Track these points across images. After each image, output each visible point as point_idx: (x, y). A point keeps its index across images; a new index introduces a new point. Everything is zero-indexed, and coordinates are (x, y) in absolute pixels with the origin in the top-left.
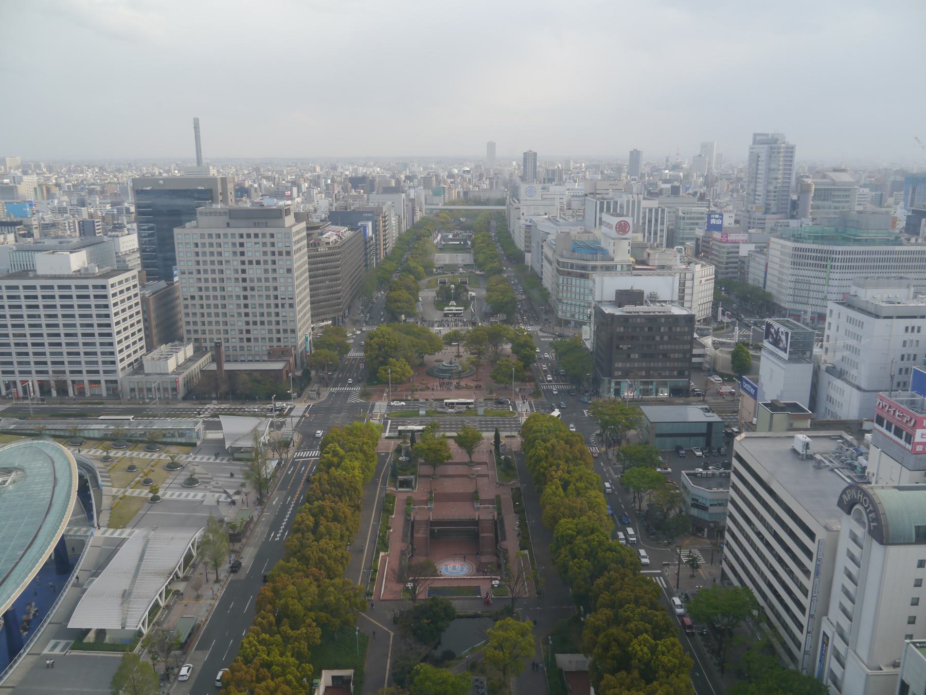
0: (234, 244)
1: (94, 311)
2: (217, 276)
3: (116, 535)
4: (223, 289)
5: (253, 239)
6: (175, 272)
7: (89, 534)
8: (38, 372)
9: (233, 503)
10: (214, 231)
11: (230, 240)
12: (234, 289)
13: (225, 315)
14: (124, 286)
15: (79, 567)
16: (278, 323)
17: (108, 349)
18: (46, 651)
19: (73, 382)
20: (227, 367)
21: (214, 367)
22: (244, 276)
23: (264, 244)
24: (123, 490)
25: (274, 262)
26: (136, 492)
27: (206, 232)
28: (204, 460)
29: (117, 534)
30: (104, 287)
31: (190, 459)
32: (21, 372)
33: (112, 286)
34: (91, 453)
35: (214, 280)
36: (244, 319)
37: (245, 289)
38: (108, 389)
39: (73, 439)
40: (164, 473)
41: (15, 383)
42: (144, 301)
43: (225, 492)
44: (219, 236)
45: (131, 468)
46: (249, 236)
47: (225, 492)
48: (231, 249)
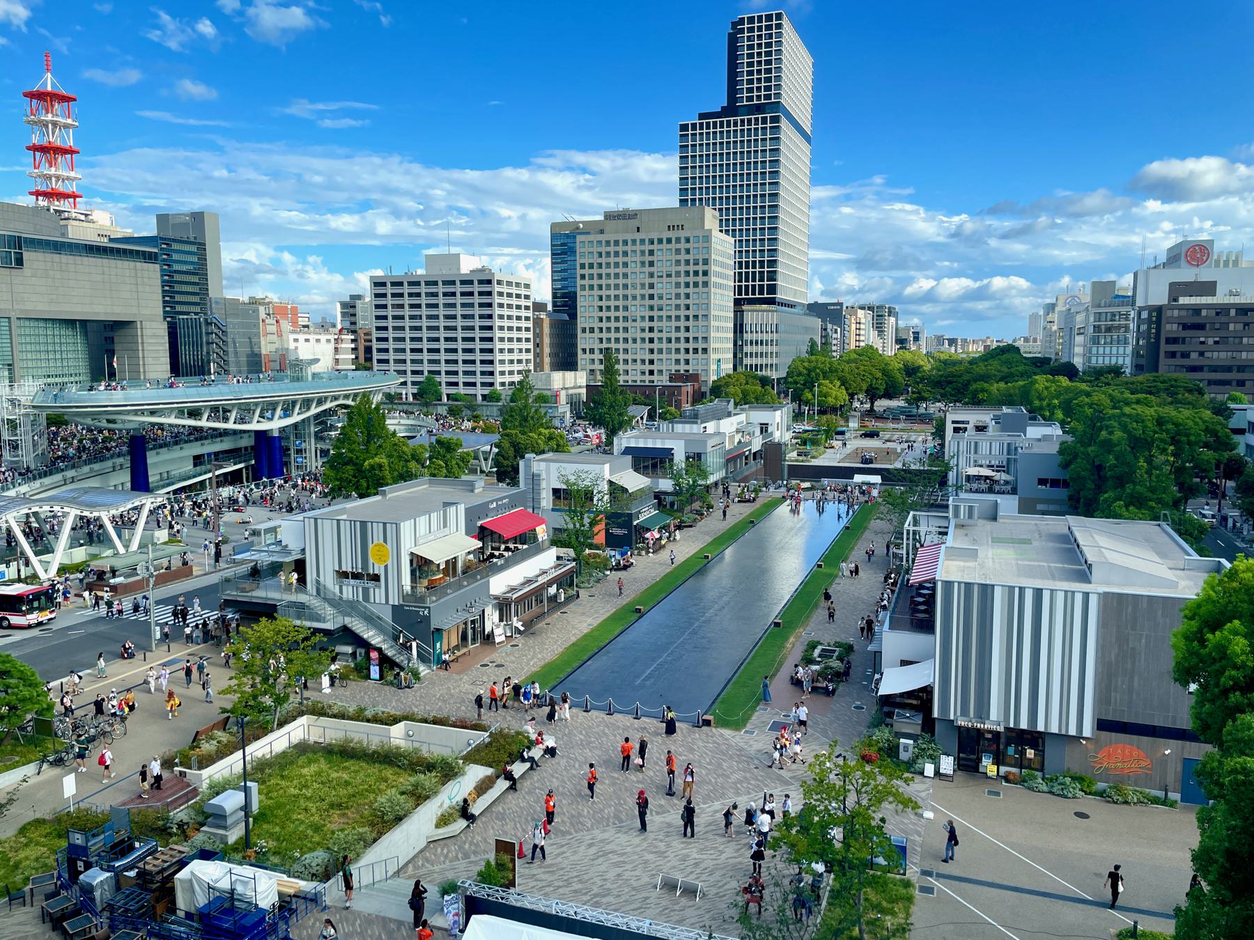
0: (643, 252)
2: (621, 292)
4: (626, 308)
5: (665, 246)
10: (620, 238)
11: (638, 248)
12: (638, 309)
13: (626, 340)
16: (687, 340)
22: (651, 292)
23: (678, 251)
25: (687, 296)
35: (617, 297)
36: (648, 346)
37: (651, 308)
44: (625, 243)
46: (660, 241)
48: (638, 258)
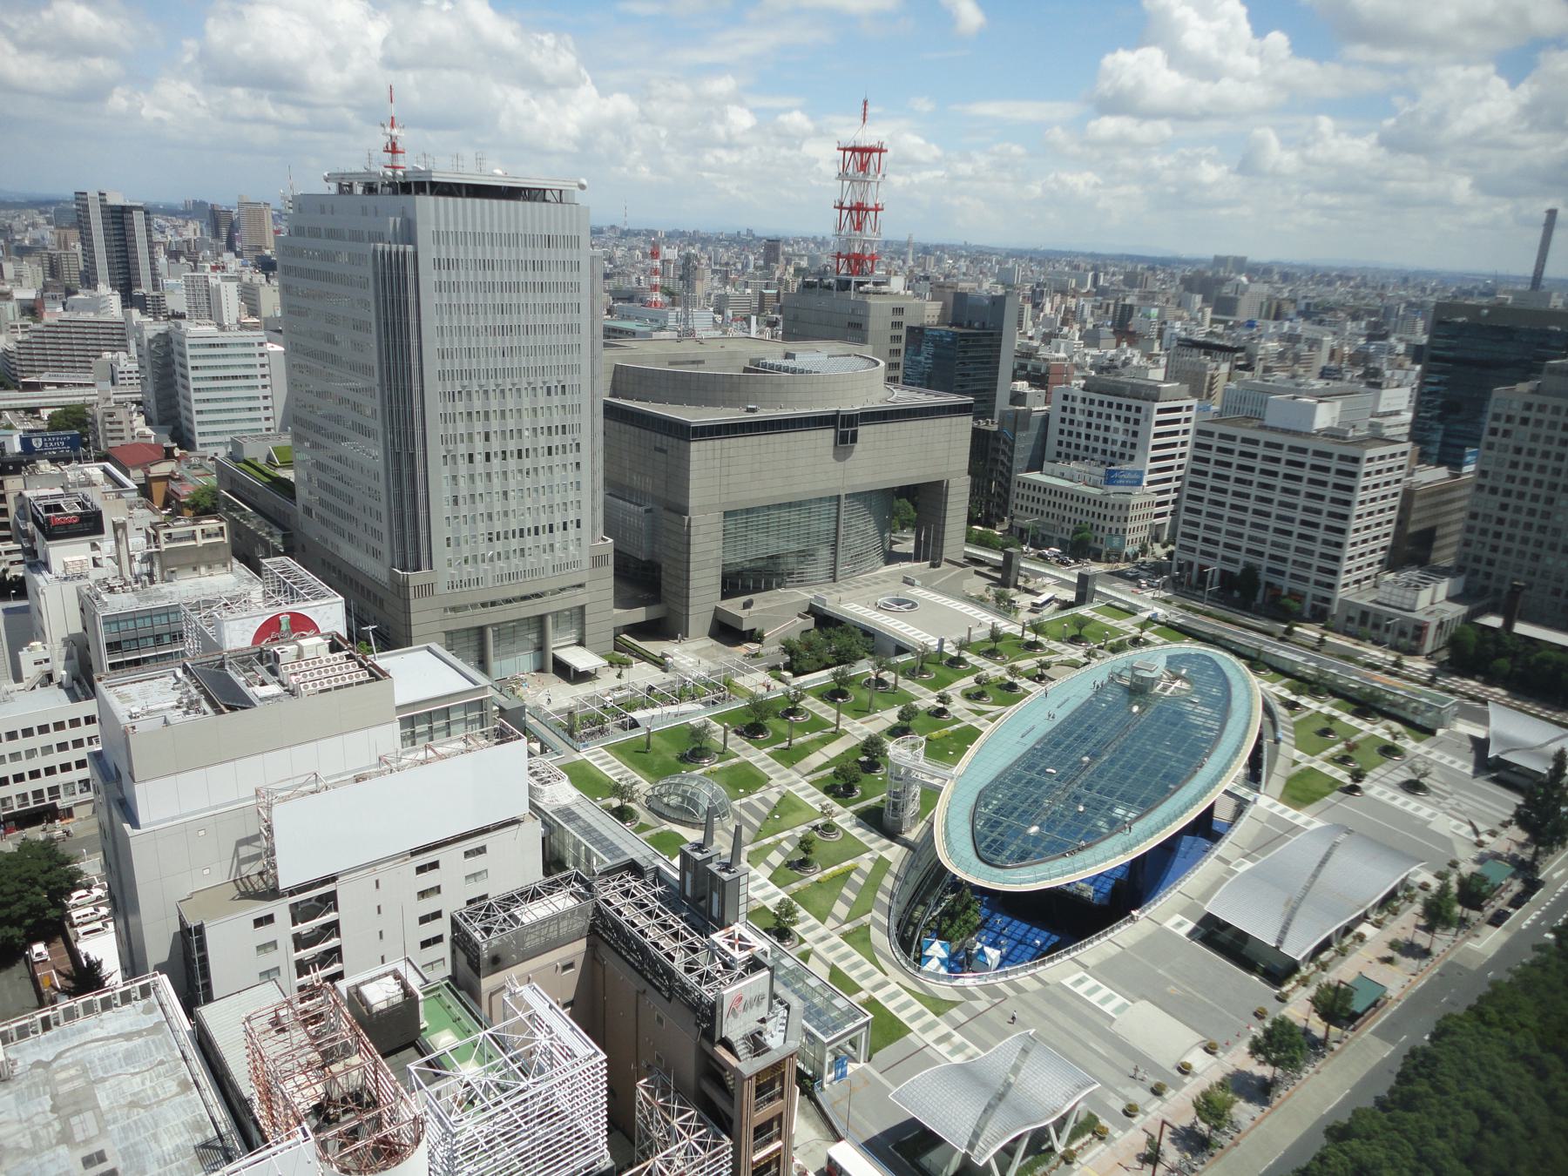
1: (1329, 492)
3: (1286, 816)
6: (1469, 458)
7: (1250, 798)
8: (1224, 558)
9: (1480, 844)
14: (1388, 463)
15: (1230, 838)
17: (1333, 551)
18: (1169, 925)
19: (1269, 585)
20: (1521, 628)
21: (1495, 621)
24: (1309, 757)
26: (1328, 769)
27: (1552, 402)
28: (1444, 761)
29: (1290, 814)
30: (1356, 460)
31: (1418, 751)
32: (1203, 553)
33: (1370, 460)
34: (1280, 689)
38: (1314, 607)
39: (1256, 662)
40: (1377, 757)
41: (1191, 564)
42: (1408, 495)
43: (1471, 824)
45: (1325, 732)
47: (1471, 824)
